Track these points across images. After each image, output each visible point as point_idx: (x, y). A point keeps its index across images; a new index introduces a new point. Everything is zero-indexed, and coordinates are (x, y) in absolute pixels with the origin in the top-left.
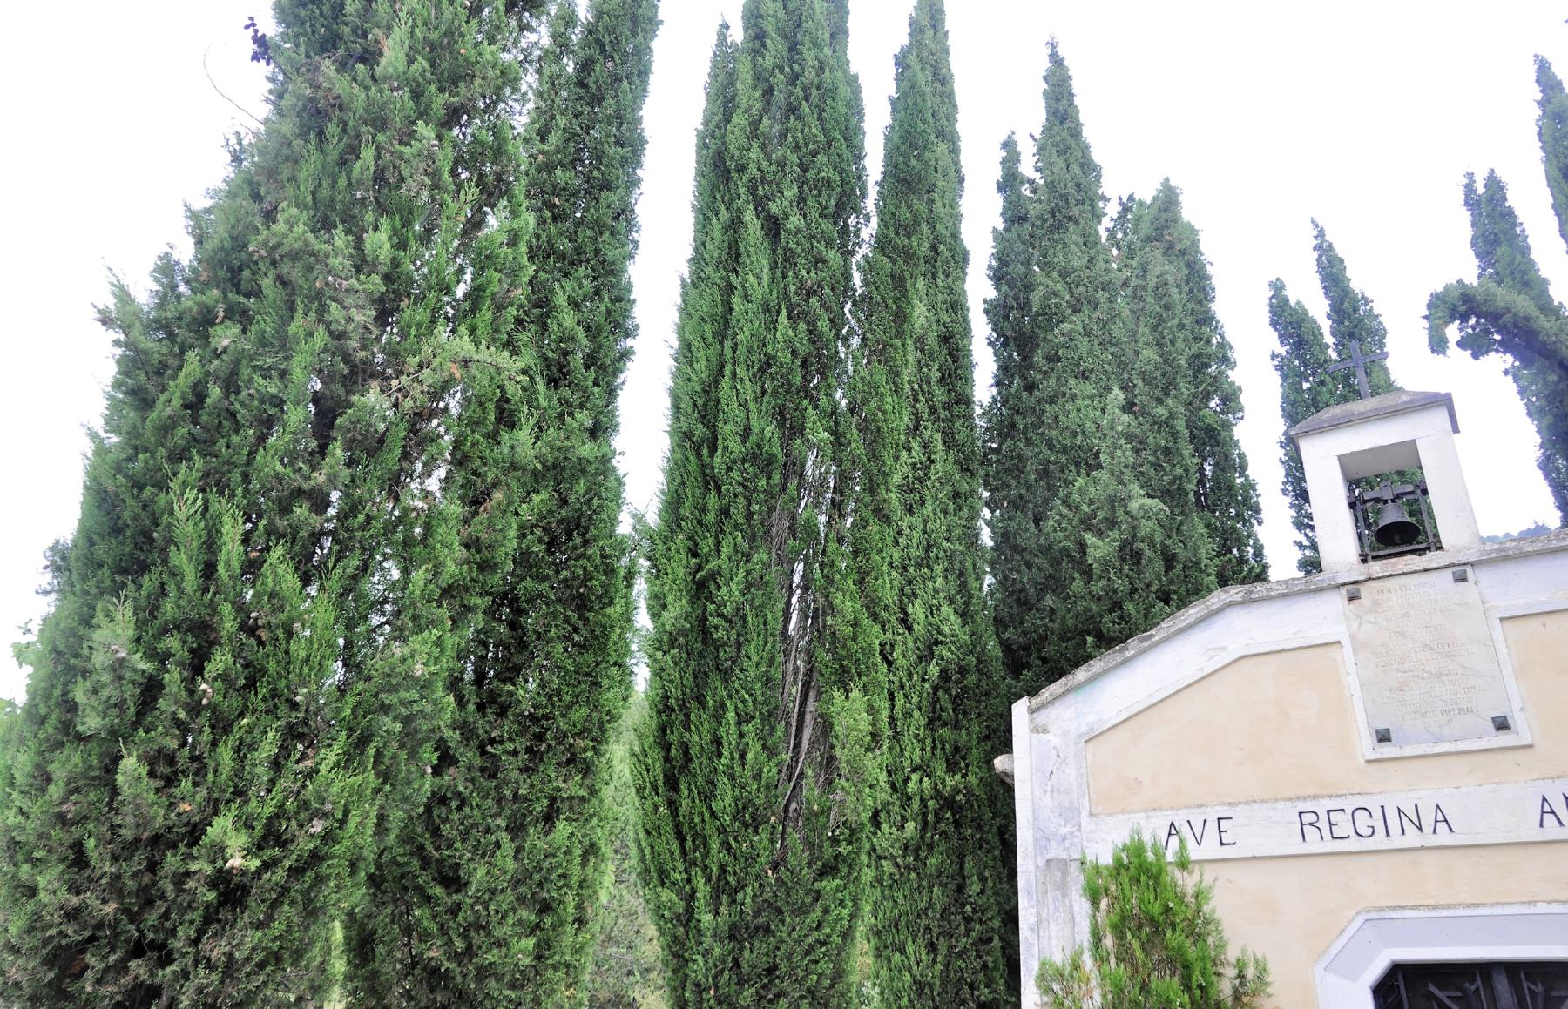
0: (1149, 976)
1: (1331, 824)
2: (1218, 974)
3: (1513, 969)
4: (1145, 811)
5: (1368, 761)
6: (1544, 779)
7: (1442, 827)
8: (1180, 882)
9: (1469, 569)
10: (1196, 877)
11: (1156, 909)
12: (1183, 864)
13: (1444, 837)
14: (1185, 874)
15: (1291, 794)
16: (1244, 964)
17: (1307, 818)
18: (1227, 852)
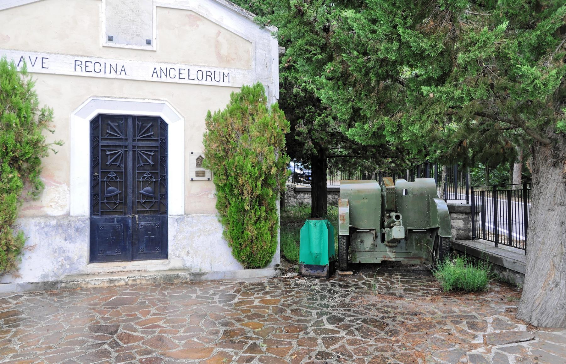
1: (86, 66)
2: (34, 113)
3: (135, 118)
4: (10, 50)
6: (156, 62)
7: (123, 72)
8: (22, 79)
10: (29, 78)
11: (9, 88)
12: (24, 72)
13: (123, 76)
14: (25, 76)
15: (73, 53)
16: (45, 111)
17: (78, 63)
18: (44, 71)
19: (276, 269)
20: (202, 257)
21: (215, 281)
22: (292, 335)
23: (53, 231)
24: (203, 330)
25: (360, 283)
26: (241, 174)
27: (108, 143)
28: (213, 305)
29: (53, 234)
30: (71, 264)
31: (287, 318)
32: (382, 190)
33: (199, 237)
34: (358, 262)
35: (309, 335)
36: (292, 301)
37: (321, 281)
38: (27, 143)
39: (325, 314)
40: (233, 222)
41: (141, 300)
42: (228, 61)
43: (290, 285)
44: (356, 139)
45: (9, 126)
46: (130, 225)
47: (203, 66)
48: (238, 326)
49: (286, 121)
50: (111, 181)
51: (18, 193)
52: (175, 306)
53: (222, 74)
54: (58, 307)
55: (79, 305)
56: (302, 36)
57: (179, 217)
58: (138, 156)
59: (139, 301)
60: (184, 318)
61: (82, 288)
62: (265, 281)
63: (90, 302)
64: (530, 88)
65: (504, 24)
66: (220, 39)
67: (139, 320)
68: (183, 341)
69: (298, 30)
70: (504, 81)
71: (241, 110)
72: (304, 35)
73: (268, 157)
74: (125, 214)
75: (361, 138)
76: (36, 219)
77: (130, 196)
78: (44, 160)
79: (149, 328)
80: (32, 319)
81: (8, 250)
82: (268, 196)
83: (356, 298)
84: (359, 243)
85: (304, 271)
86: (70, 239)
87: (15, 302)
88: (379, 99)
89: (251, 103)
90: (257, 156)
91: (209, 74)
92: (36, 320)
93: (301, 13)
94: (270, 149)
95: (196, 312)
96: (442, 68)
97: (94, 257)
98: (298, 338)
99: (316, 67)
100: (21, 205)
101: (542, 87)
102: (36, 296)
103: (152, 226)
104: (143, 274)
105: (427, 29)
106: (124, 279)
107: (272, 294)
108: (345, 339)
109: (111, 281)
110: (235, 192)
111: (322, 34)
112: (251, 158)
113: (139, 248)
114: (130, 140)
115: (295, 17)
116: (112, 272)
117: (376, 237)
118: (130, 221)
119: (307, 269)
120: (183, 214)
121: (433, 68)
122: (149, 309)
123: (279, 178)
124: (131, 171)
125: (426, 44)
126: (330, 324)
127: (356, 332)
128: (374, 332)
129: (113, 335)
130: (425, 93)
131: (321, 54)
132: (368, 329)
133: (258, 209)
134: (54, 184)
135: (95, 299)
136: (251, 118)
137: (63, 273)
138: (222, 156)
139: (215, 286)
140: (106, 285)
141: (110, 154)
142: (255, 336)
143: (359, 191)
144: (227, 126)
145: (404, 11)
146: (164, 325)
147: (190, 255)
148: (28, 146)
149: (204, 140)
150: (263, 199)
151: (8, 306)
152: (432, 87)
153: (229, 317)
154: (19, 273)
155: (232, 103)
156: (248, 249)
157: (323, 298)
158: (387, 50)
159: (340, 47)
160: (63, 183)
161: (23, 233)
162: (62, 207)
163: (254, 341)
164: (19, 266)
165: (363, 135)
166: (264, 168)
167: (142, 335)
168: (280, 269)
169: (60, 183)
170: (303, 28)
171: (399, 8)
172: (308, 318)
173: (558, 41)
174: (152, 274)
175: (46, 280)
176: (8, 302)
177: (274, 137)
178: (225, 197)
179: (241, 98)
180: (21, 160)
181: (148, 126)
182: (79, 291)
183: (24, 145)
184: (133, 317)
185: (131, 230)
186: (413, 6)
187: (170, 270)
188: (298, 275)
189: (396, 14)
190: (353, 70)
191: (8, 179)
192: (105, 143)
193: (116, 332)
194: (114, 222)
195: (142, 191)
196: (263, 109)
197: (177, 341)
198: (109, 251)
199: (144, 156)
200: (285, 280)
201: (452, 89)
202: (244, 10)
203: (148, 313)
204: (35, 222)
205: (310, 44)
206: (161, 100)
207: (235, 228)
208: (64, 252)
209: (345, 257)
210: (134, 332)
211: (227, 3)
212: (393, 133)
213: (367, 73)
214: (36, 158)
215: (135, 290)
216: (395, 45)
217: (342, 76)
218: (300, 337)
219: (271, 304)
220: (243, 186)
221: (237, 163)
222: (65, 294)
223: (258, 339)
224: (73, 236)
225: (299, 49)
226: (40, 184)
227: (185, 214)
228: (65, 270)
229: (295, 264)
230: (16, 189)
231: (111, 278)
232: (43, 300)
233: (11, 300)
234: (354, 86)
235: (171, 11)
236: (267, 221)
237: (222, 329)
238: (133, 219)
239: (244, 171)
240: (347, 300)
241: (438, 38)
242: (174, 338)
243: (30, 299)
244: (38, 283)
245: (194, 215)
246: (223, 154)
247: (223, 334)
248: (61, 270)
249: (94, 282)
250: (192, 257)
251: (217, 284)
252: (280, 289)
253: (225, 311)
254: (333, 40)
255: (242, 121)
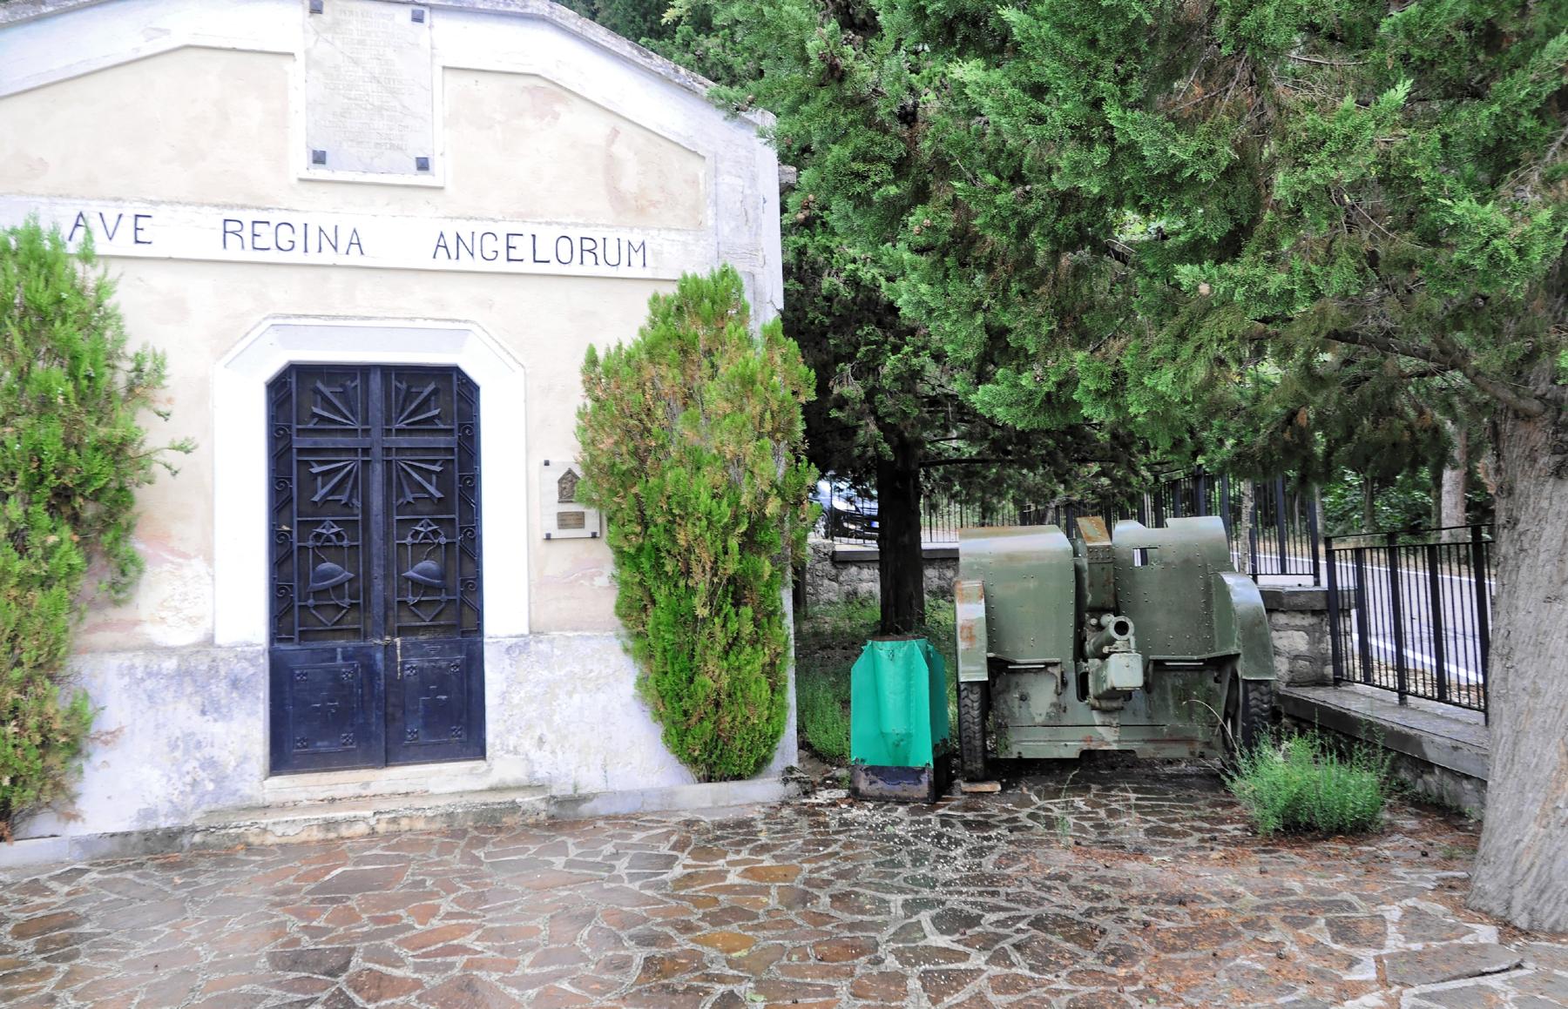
0: (29, 365)
2: (113, 367)
3: (387, 370)
5: (301, 180)
7: (355, 248)
8: (80, 274)
9: (427, 11)
10: (100, 271)
11: (45, 298)
12: (87, 257)
13: (354, 258)
14: (88, 267)
16: (143, 358)
17: (231, 226)
19: (786, 781)
20: (579, 751)
21: (616, 817)
22: (837, 968)
23: (167, 687)
24: (584, 958)
25: (1023, 814)
26: (682, 518)
27: (315, 443)
28: (613, 885)
29: (169, 696)
30: (219, 780)
31: (820, 919)
32: (1076, 553)
33: (571, 697)
34: (1015, 756)
35: (882, 968)
36: (832, 869)
37: (912, 812)
38: (97, 449)
39: (927, 904)
40: (665, 650)
41: (413, 874)
42: (641, 211)
43: (826, 825)
44: (1001, 413)
45: (45, 403)
46: (380, 666)
47: (572, 224)
48: (683, 943)
49: (803, 369)
50: (326, 547)
51: (72, 586)
52: (508, 891)
53: (624, 246)
54: (184, 900)
55: (240, 894)
56: (841, 138)
57: (515, 640)
58: (398, 476)
59: (407, 878)
60: (532, 923)
61: (249, 847)
62: (756, 814)
63: (271, 884)
64: (1479, 263)
65: (1399, 87)
66: (619, 149)
67: (409, 934)
68: (530, 991)
69: (829, 121)
70: (1406, 243)
71: (678, 343)
72: (846, 134)
73: (756, 471)
74: (365, 637)
75: (1013, 411)
76: (123, 655)
77: (378, 586)
78: (143, 496)
79: (436, 954)
80: (113, 935)
81: (46, 745)
82: (758, 577)
83: (1012, 859)
84: (1017, 702)
85: (863, 785)
86: (217, 710)
87: (67, 889)
88: (1059, 302)
89: (707, 322)
90: (726, 468)
91: (588, 245)
92: (124, 939)
93: (837, 74)
94: (762, 448)
95: (566, 908)
96: (1231, 212)
97: (282, 758)
98: (851, 974)
99: (880, 218)
100: (81, 619)
101: (1514, 258)
102: (122, 870)
103: (440, 668)
104: (418, 803)
105: (1185, 107)
106: (365, 819)
107: (778, 852)
108: (985, 975)
109: (329, 825)
110: (668, 568)
111: (899, 128)
112: (709, 473)
113: (405, 731)
114: (376, 434)
115: (821, 85)
116: (333, 800)
117: (1064, 684)
118: (379, 656)
119: (873, 778)
120: (526, 632)
121: (1205, 215)
122: (436, 902)
123: (787, 526)
124: (380, 518)
125: (1184, 148)
126: (943, 933)
127: (1015, 956)
128: (1067, 955)
129: (338, 976)
130: (1186, 283)
131: (894, 182)
132: (1048, 946)
133: (732, 614)
134: (170, 558)
135: (287, 877)
136: (706, 362)
137: (197, 805)
138: (629, 471)
139: (618, 830)
140: (317, 835)
141: (323, 474)
142: (731, 972)
143: (1011, 557)
144: (641, 386)
145: (1120, 61)
146: (478, 946)
147: (547, 747)
148: (99, 456)
149: (579, 427)
150: (744, 587)
151: (45, 900)
152: (1206, 265)
153: (659, 920)
154: (77, 807)
155: (653, 324)
156: (708, 725)
157: (919, 858)
158: (1077, 169)
159: (947, 164)
160: (195, 557)
161: (86, 696)
162: (192, 621)
163: (730, 987)
164: (75, 788)
165: (1017, 403)
166: (746, 499)
167: (416, 976)
168: (797, 780)
169: (185, 556)
170: (845, 115)
171: (1106, 52)
172: (879, 919)
173: (1554, 129)
174: (441, 803)
175: (150, 826)
176: (47, 889)
177: (772, 413)
178: (641, 584)
179: (679, 308)
180: (81, 495)
181: (425, 393)
182: (241, 855)
183: (87, 452)
184: (392, 925)
185: (383, 681)
186: (1144, 47)
187: (492, 789)
188: (848, 797)
189: (1098, 69)
190: (986, 226)
191: (44, 548)
192: (307, 442)
193: (344, 967)
194: (334, 659)
195: (410, 573)
196: (740, 338)
197: (515, 991)
198: (322, 740)
199: (416, 476)
200: (812, 812)
201: (1260, 271)
202: (682, 71)
203: (433, 912)
204: (120, 666)
205: (865, 157)
206: (459, 321)
207: (669, 668)
208: (199, 745)
209: (978, 743)
210: (393, 966)
211: (635, 52)
212: (1100, 395)
213: (1023, 232)
214: (121, 489)
215: (398, 846)
216: (1100, 156)
217: (954, 242)
218: (858, 971)
219: (773, 881)
220: (689, 550)
221: (670, 489)
222: (203, 864)
223: (740, 980)
224: (223, 702)
225: (836, 172)
226: (133, 560)
227: (531, 632)
228: (203, 796)
229: (839, 766)
230: (68, 574)
231: (330, 815)
232: (142, 881)
233: (53, 885)
234: (989, 268)
235: (481, 78)
236: (759, 647)
237: (639, 955)
238: (389, 649)
239: (690, 510)
240: (988, 864)
241: (1218, 131)
242: (507, 984)
243: (107, 881)
244: (127, 835)
245: (555, 634)
246: (634, 463)
247: (644, 968)
248: (192, 798)
249: (283, 829)
250: (553, 752)
251: (623, 826)
252: (799, 837)
253: (648, 901)
254: (928, 143)
255: (683, 372)
